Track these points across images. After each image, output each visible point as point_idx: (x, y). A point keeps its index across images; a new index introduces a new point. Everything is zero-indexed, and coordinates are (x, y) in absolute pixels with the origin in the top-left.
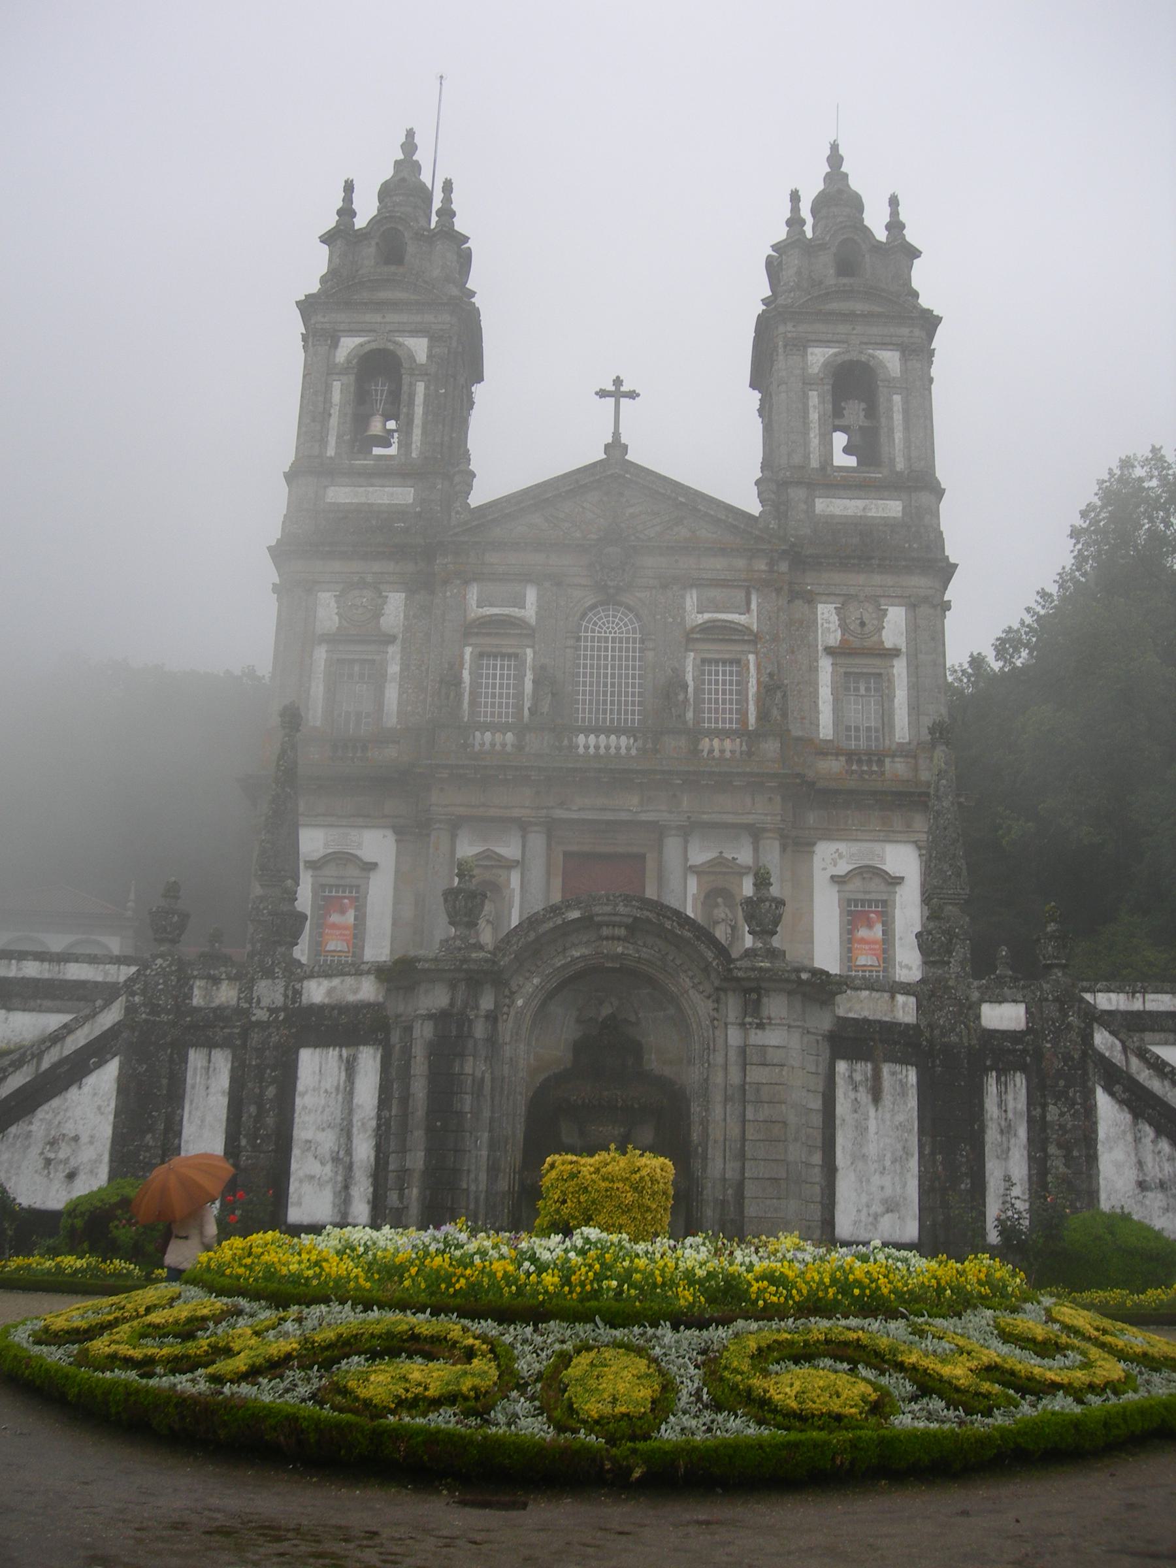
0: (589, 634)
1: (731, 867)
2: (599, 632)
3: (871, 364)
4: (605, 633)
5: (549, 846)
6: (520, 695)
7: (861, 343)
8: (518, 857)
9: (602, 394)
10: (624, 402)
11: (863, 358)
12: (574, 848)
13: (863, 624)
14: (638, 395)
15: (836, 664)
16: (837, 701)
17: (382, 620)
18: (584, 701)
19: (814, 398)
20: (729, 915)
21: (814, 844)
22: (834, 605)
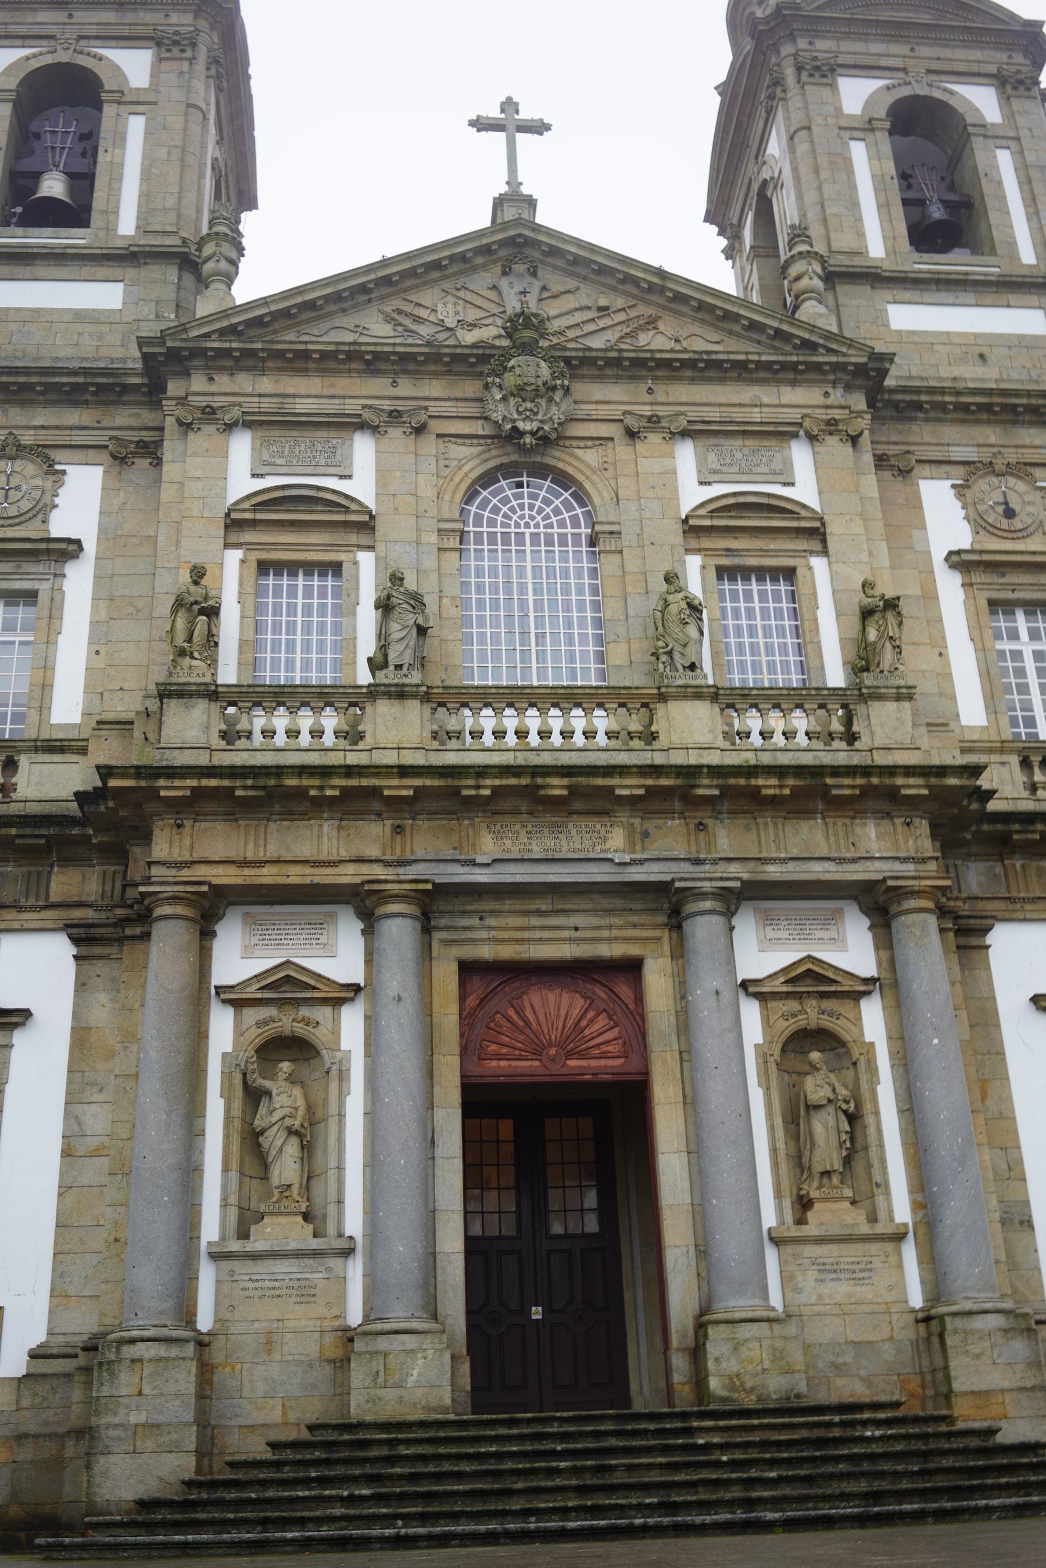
0: (485, 529)
1: (834, 982)
2: (503, 525)
3: (952, 102)
4: (517, 525)
5: (426, 953)
6: (347, 645)
7: (929, 72)
8: (357, 976)
9: (480, 124)
10: (521, 138)
11: (937, 94)
12: (486, 952)
13: (1010, 513)
14: (547, 127)
15: (971, 585)
16: (982, 650)
17: (55, 517)
18: (483, 653)
19: (858, 151)
20: (843, 1092)
21: (986, 930)
22: (949, 483)
